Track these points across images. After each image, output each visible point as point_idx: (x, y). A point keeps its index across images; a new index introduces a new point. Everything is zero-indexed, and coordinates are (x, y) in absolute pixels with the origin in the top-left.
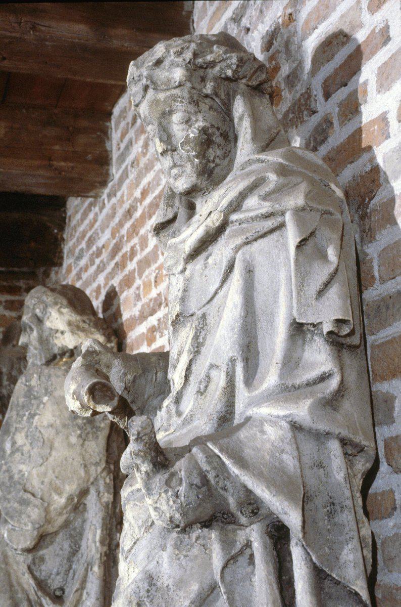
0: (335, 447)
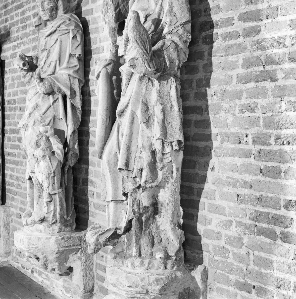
0: (77, 80)
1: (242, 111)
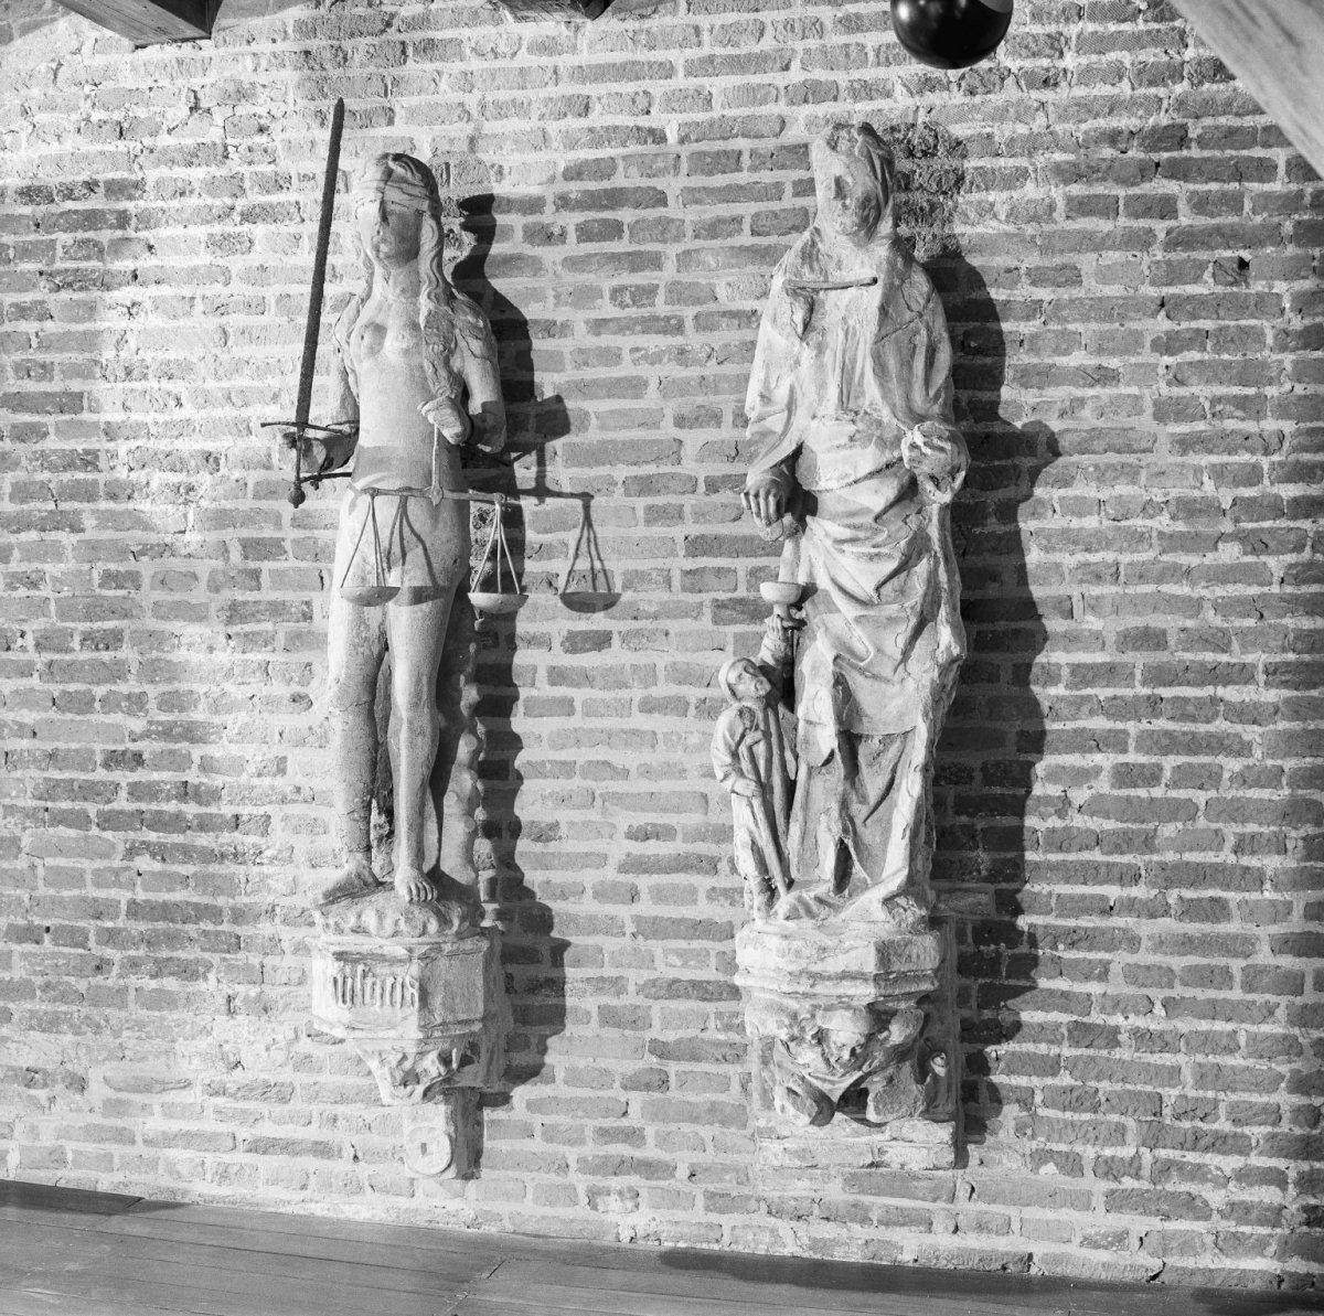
1: (11, 587)
